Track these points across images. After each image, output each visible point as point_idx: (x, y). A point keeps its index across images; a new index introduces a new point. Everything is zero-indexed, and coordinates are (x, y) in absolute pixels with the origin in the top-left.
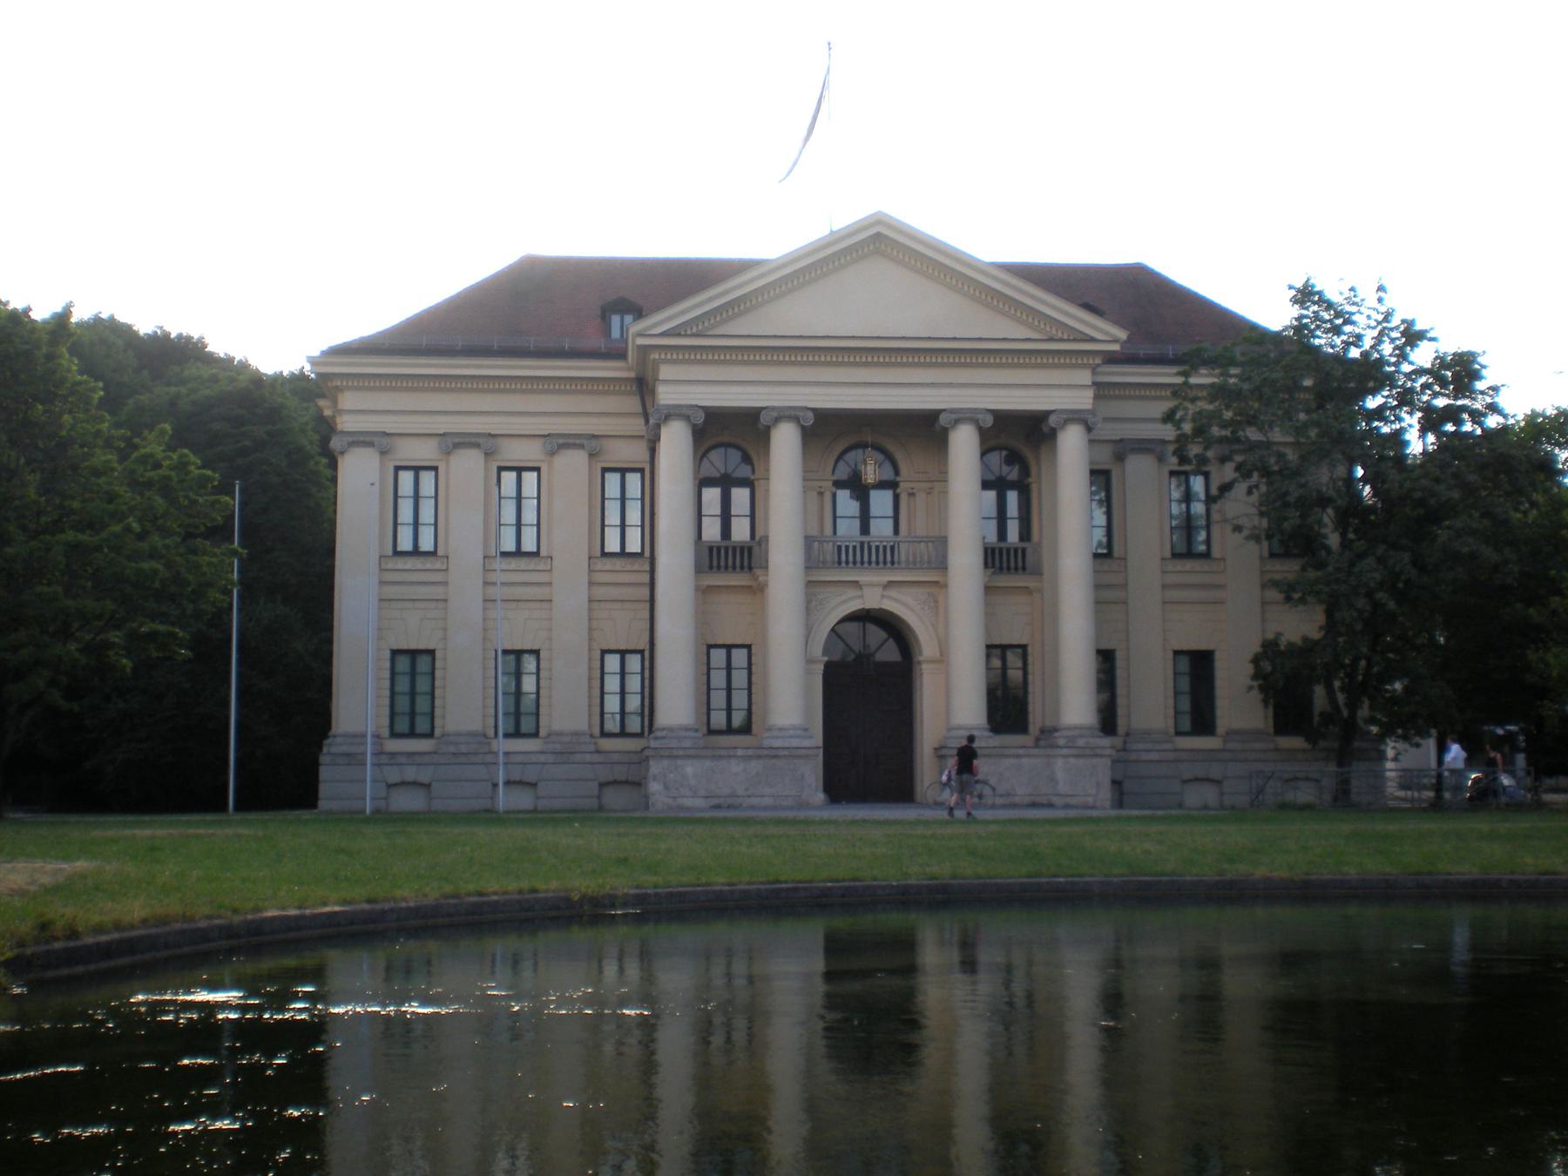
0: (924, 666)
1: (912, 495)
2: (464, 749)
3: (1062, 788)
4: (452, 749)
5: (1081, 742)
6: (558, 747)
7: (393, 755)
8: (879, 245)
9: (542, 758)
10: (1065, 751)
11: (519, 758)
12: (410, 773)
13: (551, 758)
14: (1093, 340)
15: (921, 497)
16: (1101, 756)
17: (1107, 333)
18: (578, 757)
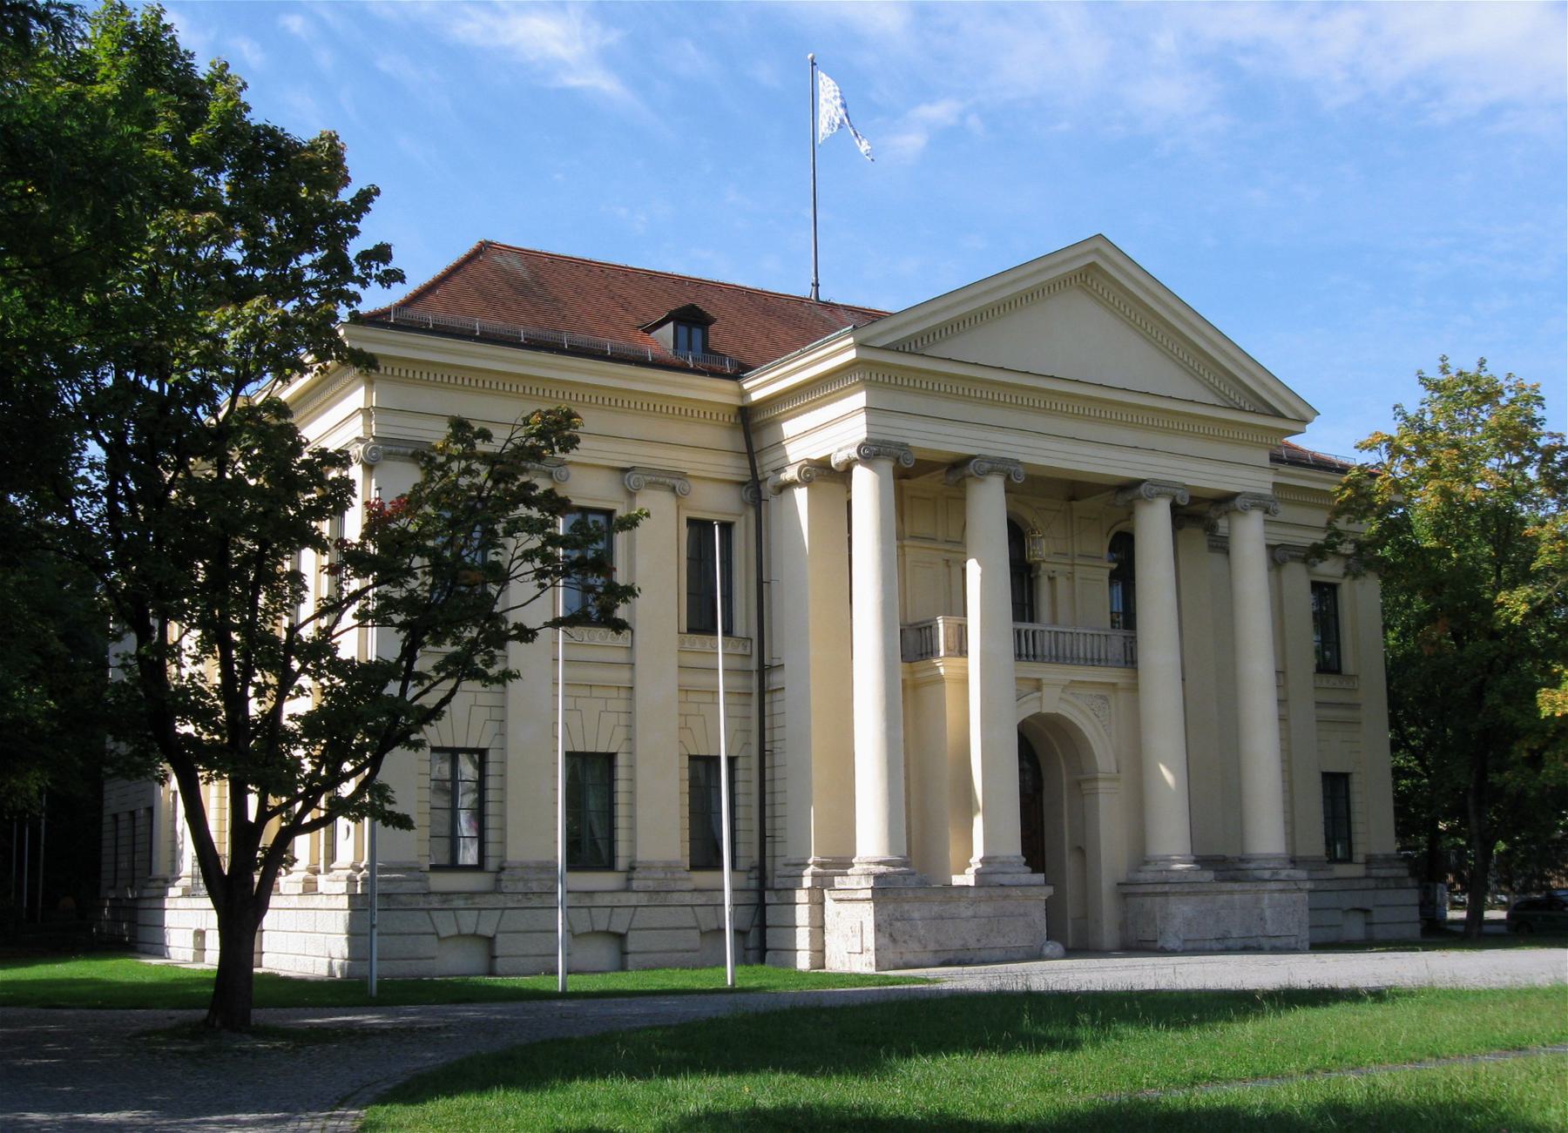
0: (1101, 785)
1: (1052, 579)
2: (535, 887)
3: (1271, 928)
4: (520, 887)
5: (1283, 874)
6: (651, 884)
7: (446, 895)
8: (1095, 275)
9: (633, 899)
10: (1273, 886)
11: (607, 900)
12: (468, 922)
13: (643, 899)
14: (1282, 416)
15: (1061, 583)
16: (1300, 890)
17: (1295, 411)
18: (675, 898)
